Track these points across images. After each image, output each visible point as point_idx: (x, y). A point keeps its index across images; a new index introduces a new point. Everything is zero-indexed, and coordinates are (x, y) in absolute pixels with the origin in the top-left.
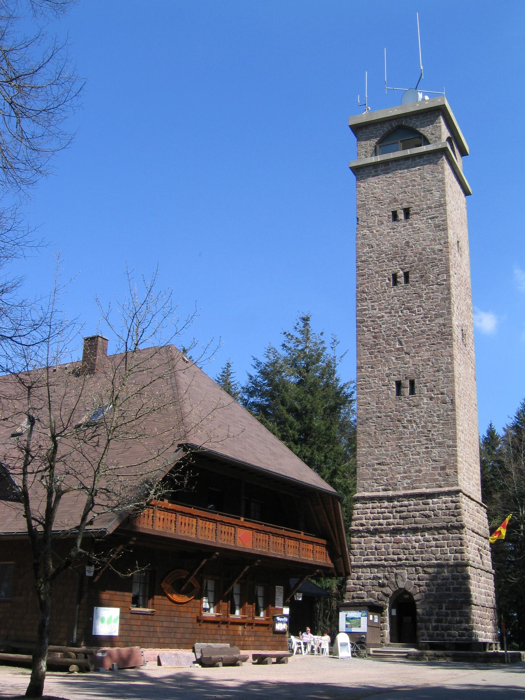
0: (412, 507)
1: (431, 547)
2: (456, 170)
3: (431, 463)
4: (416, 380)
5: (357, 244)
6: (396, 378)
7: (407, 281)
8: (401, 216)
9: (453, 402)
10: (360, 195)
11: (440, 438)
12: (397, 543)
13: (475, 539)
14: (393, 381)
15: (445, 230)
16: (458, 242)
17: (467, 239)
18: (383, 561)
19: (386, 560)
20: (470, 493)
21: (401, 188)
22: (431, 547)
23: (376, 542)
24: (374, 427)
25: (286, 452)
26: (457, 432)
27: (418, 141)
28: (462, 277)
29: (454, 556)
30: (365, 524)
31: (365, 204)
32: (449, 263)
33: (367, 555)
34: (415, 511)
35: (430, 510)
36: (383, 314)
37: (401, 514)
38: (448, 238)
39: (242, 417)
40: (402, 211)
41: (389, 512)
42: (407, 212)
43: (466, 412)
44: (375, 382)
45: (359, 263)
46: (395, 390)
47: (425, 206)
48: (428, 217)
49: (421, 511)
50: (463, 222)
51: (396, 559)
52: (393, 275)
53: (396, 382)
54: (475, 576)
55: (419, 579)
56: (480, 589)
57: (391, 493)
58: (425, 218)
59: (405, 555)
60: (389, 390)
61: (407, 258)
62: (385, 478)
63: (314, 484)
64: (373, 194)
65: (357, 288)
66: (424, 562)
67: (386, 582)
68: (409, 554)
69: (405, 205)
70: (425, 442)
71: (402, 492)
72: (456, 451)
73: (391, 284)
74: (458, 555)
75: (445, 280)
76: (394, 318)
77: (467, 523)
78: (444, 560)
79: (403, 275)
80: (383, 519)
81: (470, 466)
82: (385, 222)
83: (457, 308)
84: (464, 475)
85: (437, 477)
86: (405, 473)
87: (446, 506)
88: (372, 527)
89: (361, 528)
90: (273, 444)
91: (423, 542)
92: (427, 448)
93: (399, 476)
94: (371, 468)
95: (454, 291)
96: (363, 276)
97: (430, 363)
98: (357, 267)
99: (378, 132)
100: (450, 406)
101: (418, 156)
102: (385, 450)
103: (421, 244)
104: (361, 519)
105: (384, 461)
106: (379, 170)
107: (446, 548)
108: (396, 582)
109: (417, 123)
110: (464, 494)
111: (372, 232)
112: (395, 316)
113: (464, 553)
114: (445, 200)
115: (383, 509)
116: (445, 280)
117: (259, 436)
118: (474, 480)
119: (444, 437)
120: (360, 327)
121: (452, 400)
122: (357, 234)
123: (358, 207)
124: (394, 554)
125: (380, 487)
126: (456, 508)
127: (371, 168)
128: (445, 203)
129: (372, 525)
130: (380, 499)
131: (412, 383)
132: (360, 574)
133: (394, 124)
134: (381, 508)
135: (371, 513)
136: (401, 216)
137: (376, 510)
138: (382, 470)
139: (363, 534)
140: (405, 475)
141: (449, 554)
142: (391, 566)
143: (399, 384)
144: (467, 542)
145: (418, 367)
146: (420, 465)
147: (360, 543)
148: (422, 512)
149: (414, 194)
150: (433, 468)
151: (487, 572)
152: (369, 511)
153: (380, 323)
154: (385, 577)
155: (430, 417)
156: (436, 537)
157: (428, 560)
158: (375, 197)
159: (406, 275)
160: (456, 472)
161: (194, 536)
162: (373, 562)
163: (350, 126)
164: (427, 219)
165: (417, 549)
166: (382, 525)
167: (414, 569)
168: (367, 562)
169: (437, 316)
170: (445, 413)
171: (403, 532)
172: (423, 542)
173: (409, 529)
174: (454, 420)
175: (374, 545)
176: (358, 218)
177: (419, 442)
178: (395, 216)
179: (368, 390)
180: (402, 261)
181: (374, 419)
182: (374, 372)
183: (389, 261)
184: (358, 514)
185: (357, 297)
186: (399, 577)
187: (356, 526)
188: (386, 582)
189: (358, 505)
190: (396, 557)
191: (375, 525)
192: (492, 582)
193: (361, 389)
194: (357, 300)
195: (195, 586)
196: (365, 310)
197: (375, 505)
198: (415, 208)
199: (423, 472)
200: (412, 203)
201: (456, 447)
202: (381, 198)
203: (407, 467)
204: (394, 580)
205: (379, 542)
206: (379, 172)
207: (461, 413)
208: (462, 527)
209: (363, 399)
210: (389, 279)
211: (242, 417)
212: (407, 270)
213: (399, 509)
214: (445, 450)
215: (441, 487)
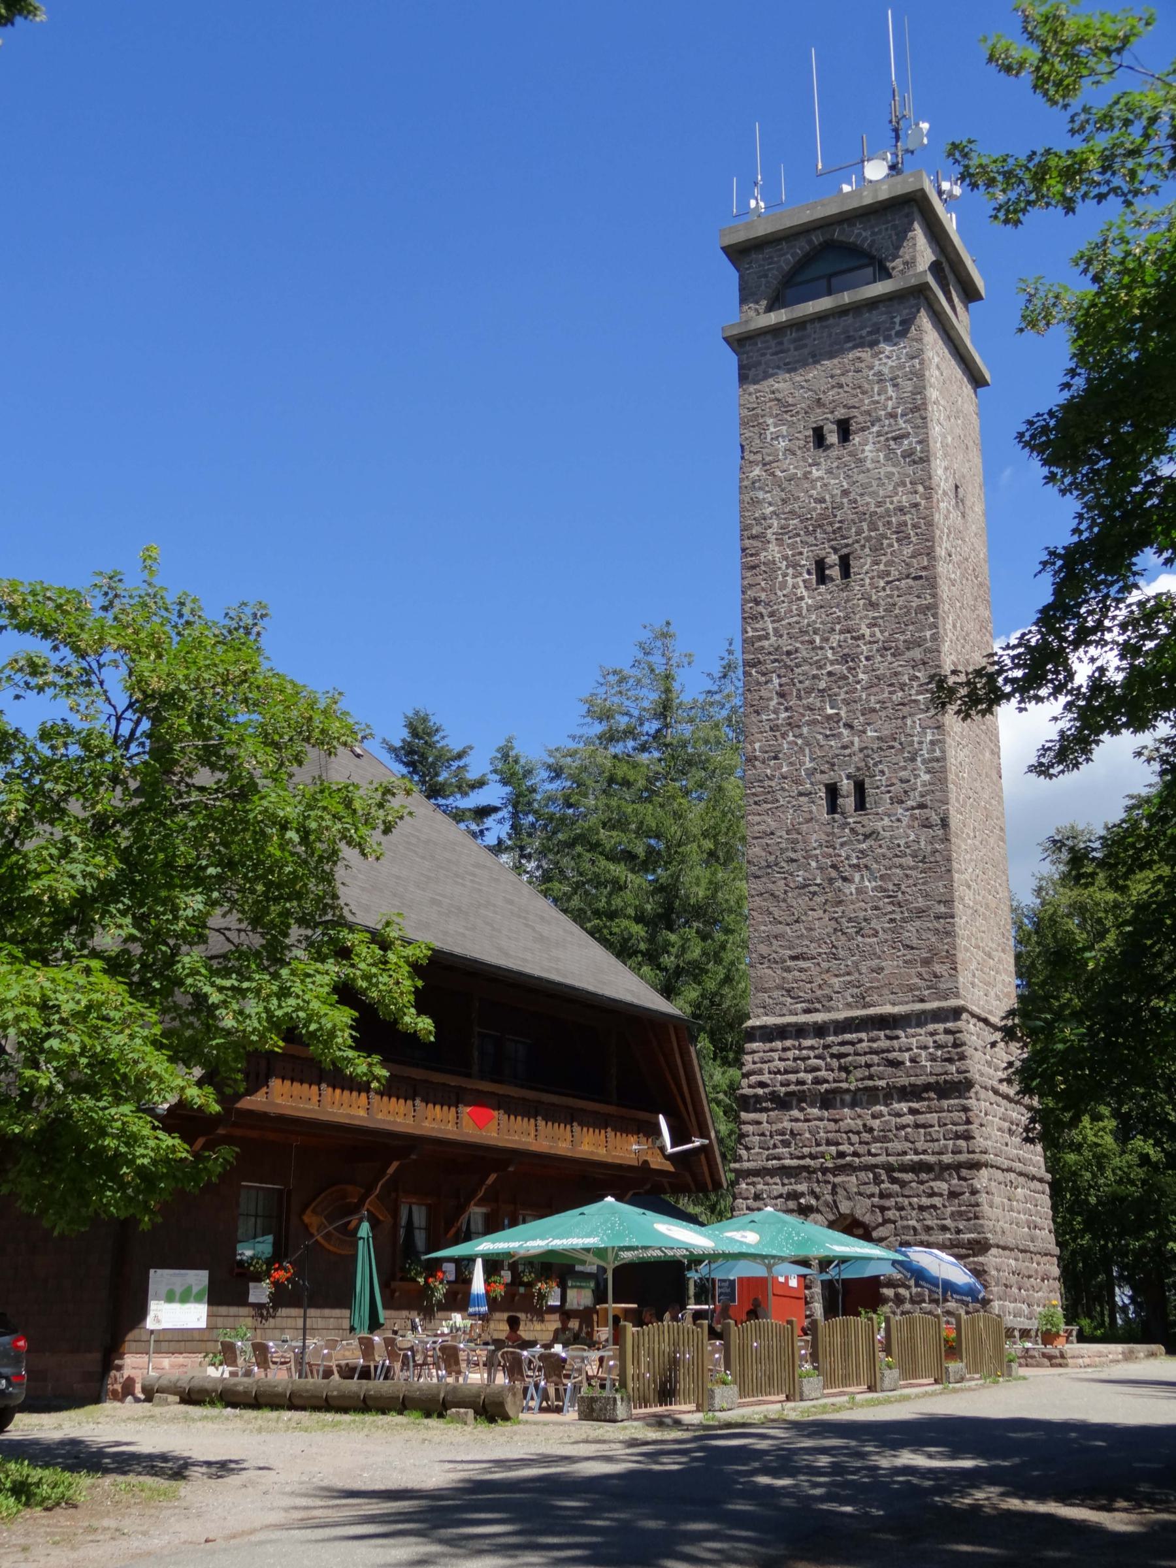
0: (864, 1044)
1: (904, 1127)
2: (952, 333)
3: (903, 952)
4: (867, 780)
5: (742, 502)
6: (825, 778)
7: (846, 572)
8: (833, 438)
9: (945, 823)
10: (747, 396)
11: (920, 899)
12: (836, 1121)
13: (1003, 1110)
14: (821, 783)
15: (925, 460)
16: (957, 487)
17: (979, 479)
18: (808, 1160)
19: (813, 1157)
20: (990, 1012)
21: (832, 377)
22: (904, 1127)
23: (791, 1121)
24: (783, 881)
25: (572, 933)
26: (955, 885)
27: (869, 271)
28: (967, 559)
29: (954, 1145)
30: (769, 1082)
31: (757, 415)
32: (933, 531)
33: (775, 1146)
34: (871, 1053)
35: (900, 1050)
36: (798, 645)
37: (842, 1061)
38: (930, 478)
39: (477, 865)
40: (835, 427)
41: (816, 1057)
42: (845, 429)
43: (977, 843)
44: (783, 789)
45: (747, 541)
46: (824, 802)
47: (883, 413)
49: (883, 1051)
50: (971, 444)
51: (834, 1153)
52: (817, 562)
53: (827, 786)
54: (1003, 1186)
55: (882, 1196)
56: (1015, 1214)
57: (819, 1017)
58: (882, 439)
59: (852, 1144)
60: (813, 802)
62: (809, 986)
63: (628, 998)
64: (773, 392)
65: (743, 593)
66: (890, 1158)
67: (813, 1202)
68: (860, 1143)
69: (841, 413)
70: (890, 908)
71: (841, 1015)
72: (953, 925)
73: (814, 581)
74: (962, 1143)
76: (820, 652)
77: (982, 1075)
78: (933, 1153)
79: (837, 562)
80: (806, 1071)
81: (990, 956)
82: (799, 452)
83: (954, 626)
84: (974, 976)
85: (917, 980)
86: (849, 974)
87: (935, 1042)
88: (783, 1089)
89: (760, 1091)
90: (542, 918)
91: (887, 1118)
92: (892, 920)
93: (835, 980)
94: (779, 966)
95: (944, 590)
96: (754, 567)
97: (896, 744)
98: (743, 550)
100: (940, 832)
101: (867, 305)
102: (806, 929)
103: (873, 494)
104: (760, 1072)
105: (805, 950)
106: (785, 340)
107: (937, 1128)
108: (835, 1201)
109: (864, 234)
110: (973, 1015)
111: (773, 474)
112: (822, 648)
113: (974, 1138)
114: (924, 398)
115: (804, 1052)
116: (925, 568)
117: (511, 902)
118: (1000, 986)
119: (927, 896)
120: (750, 675)
121: (942, 820)
122: (742, 480)
123: (744, 423)
124: (829, 1143)
125: (799, 1006)
126: (956, 1045)
127: (769, 337)
128: (924, 404)
129: (782, 1085)
130: (800, 1031)
131: (860, 788)
132: (760, 1187)
133: (817, 239)
134: (800, 1048)
135: (781, 1059)
136: (833, 438)
137: (790, 1054)
138: (801, 970)
139: (764, 1105)
140: (848, 978)
141: (942, 1142)
142: (825, 1171)
143: (833, 791)
144: (982, 1114)
145: (870, 752)
146: (879, 957)
147: (759, 1123)
148: (885, 1055)
149: (860, 387)
150: (905, 962)
151: (1033, 1178)
152: (776, 1055)
153: (792, 664)
154: (812, 1193)
155: (897, 856)
156: (915, 1105)
157: (899, 1155)
158: (778, 400)
159: (845, 565)
160: (955, 969)
161: (362, 1113)
162: (787, 1162)
164: (887, 440)
165: (876, 1133)
166: (803, 1083)
167: (871, 1176)
168: (774, 1162)
169: (910, 645)
170: (929, 848)
171: (848, 1098)
172: (887, 1118)
173: (859, 1089)
174: (949, 860)
175: (787, 1125)
176: (742, 447)
177: (876, 908)
178: (819, 438)
179: (769, 806)
180: (834, 532)
181: (783, 864)
182: (780, 767)
183: (808, 533)
184: (754, 1063)
185: (743, 611)
186: (839, 1190)
187: (750, 1086)
188: (813, 1202)
189: (755, 1045)
190: (833, 1149)
191: (788, 1085)
192: (1046, 1200)
193: (756, 803)
194: (744, 618)
195: (381, 1218)
196: (760, 638)
197: (788, 1043)
198: (860, 419)
199: (886, 972)
200: (854, 407)
201: (953, 917)
202: (790, 400)
203: (853, 962)
204: (829, 1198)
205: (797, 1120)
206: (786, 345)
207: (964, 847)
208: (969, 1084)
209: (758, 824)
210: (809, 573)
211: (477, 865)
212: (845, 551)
213: (835, 1050)
214: (929, 925)
215: (922, 1001)
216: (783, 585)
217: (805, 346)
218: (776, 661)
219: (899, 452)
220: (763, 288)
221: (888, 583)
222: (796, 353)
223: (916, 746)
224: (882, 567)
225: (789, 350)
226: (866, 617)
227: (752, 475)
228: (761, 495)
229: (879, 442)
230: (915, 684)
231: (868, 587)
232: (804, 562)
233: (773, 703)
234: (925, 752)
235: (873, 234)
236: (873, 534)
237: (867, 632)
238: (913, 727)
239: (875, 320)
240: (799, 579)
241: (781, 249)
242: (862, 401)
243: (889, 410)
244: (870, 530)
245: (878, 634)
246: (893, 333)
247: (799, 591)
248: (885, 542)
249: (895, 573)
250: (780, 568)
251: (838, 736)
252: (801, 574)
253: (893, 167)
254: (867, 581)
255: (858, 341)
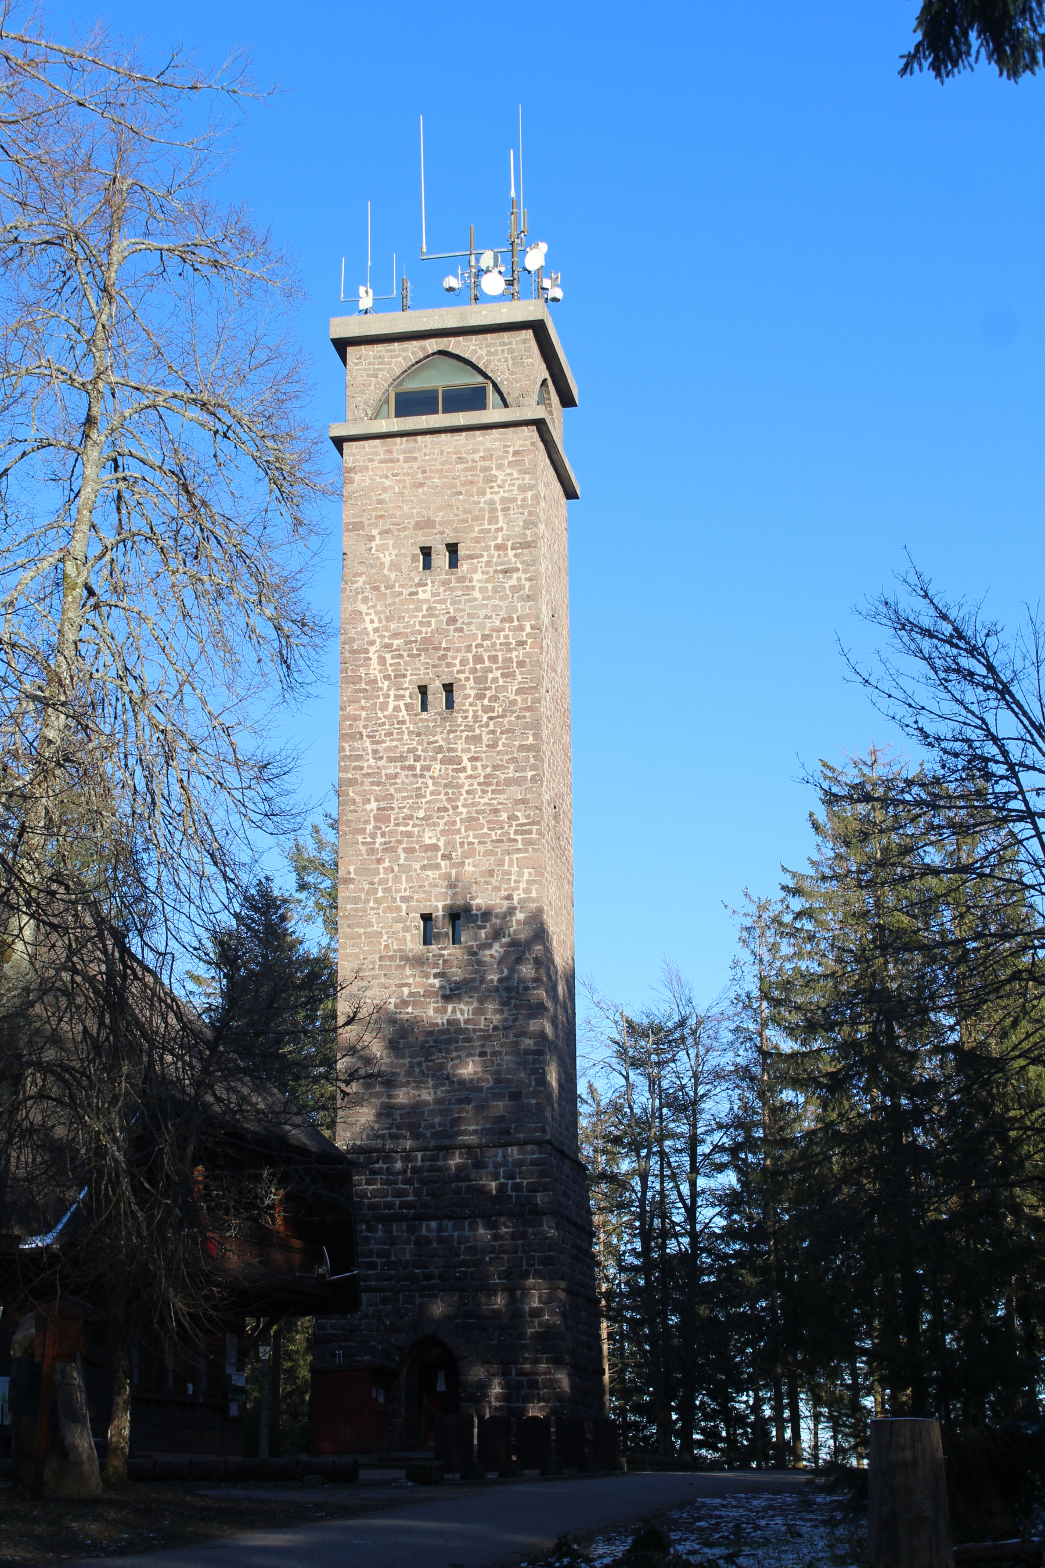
2: (555, 456)
48: (499, 568)
61: (450, 654)
75: (529, 709)
76: (420, 780)
99: (394, 360)
112: (422, 776)
116: (529, 709)
163: (333, 340)
164: (496, 571)
180: (439, 659)
185: (341, 727)
196: (359, 757)
216: (384, 706)
217: (415, 459)
218: (372, 783)
219: (507, 585)
220: (373, 387)
221: (491, 718)
222: (406, 465)
223: (513, 884)
224: (486, 702)
225: (398, 460)
226: (469, 750)
227: (355, 586)
228: (363, 608)
229: (487, 573)
230: (514, 823)
231: (470, 719)
232: (406, 685)
233: (369, 828)
234: (521, 892)
235: (489, 353)
236: (478, 667)
237: (469, 765)
238: (511, 865)
239: (488, 446)
240: (401, 703)
241: (394, 351)
242: (472, 527)
243: (499, 541)
244: (475, 662)
245: (480, 770)
246: (506, 462)
247: (401, 714)
248: (490, 676)
249: (499, 710)
250: (381, 689)
251: (437, 866)
252: (403, 697)
253: (510, 283)
254: (471, 714)
255: (470, 464)
